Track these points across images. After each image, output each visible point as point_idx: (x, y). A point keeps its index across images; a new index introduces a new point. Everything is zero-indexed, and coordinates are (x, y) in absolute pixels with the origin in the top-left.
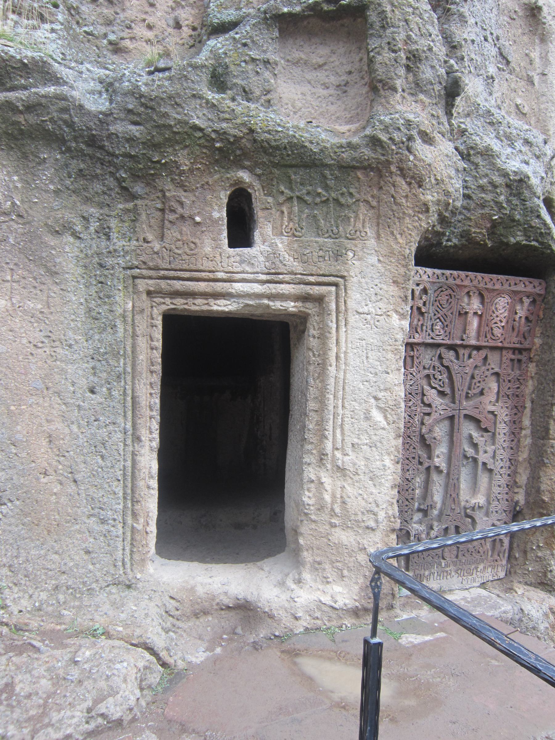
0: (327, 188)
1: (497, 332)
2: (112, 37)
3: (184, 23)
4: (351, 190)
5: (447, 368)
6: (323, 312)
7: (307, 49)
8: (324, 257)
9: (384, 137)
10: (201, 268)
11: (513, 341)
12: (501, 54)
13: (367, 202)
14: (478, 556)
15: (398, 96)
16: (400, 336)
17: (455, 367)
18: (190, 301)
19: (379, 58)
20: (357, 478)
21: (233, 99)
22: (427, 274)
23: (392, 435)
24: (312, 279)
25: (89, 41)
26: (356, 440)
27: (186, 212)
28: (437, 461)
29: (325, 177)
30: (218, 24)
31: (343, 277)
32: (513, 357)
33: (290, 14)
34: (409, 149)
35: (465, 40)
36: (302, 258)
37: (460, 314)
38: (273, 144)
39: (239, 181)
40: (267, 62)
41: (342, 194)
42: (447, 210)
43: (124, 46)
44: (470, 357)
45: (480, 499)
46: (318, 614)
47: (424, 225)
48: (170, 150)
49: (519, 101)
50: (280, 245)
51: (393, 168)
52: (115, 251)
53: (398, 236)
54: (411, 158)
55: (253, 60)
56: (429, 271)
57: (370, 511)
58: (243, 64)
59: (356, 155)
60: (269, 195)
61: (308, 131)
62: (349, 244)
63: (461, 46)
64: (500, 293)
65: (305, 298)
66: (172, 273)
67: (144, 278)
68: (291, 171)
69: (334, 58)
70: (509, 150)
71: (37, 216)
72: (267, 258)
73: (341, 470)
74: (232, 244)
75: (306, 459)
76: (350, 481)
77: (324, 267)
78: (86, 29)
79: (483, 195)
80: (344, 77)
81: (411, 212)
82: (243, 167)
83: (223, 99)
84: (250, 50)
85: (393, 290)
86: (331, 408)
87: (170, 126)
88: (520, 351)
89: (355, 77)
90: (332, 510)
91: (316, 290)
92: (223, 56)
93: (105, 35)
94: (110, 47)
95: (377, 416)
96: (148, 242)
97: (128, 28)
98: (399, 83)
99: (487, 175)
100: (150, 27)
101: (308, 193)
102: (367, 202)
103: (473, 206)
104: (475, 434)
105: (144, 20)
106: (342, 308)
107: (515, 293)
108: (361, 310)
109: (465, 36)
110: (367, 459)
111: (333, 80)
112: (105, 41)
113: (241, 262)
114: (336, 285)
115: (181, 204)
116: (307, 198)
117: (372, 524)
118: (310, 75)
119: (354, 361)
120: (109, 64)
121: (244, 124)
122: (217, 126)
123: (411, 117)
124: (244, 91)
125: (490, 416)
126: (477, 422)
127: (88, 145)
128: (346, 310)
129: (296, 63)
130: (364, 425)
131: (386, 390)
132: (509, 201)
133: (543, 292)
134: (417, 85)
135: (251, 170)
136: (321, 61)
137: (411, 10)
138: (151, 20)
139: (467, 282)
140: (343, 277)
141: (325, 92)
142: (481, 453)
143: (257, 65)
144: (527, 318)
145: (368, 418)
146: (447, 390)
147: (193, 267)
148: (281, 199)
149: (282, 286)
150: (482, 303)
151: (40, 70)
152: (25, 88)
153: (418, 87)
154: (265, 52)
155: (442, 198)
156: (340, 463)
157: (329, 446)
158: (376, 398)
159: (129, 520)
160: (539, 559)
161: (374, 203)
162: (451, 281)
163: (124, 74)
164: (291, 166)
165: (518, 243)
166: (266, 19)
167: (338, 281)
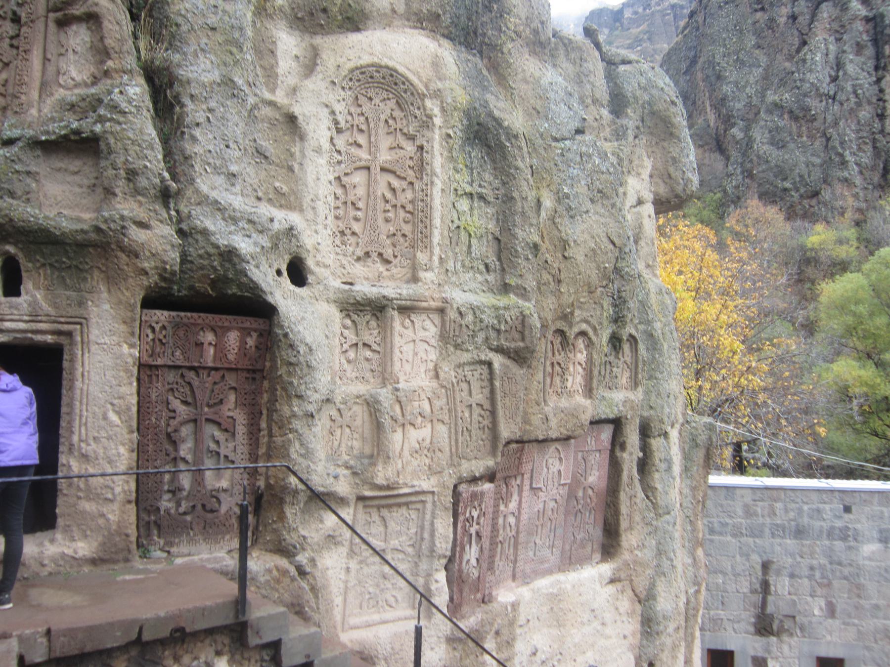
0: (69, 258)
1: (231, 357)
4: (87, 260)
5: (189, 383)
6: (72, 343)
7: (66, 161)
8: (70, 305)
9: (104, 227)
11: (245, 364)
12: (258, 152)
13: (99, 268)
14: (224, 528)
15: (118, 199)
17: (196, 383)
19: (105, 174)
22: (161, 316)
23: (125, 431)
24: (62, 320)
26: (96, 434)
28: (182, 453)
29: (67, 251)
31: (85, 319)
32: (248, 375)
33: (47, 141)
34: (124, 235)
35: (196, 154)
36: (56, 306)
37: (196, 344)
38: (27, 229)
39: (7, 252)
40: (28, 173)
41: (81, 263)
42: (166, 272)
44: (209, 375)
45: (224, 484)
46: (62, 563)
47: (146, 283)
49: (277, 184)
50: (38, 296)
51: (113, 246)
53: (125, 291)
54: (126, 240)
55: (18, 172)
56: (166, 313)
57: (107, 487)
59: (85, 237)
60: (30, 261)
61: (55, 220)
62: (87, 296)
63: (191, 157)
64: (229, 329)
65: (59, 333)
69: (86, 168)
70: (233, 228)
72: (30, 305)
73: (85, 457)
74: (7, 294)
76: (92, 464)
77: (72, 311)
80: (93, 181)
81: (132, 274)
82: (9, 243)
84: (16, 164)
85: (123, 328)
86: (78, 411)
88: (254, 371)
90: (78, 486)
91: (66, 327)
95: (113, 417)
98: (117, 191)
99: (204, 247)
101: (57, 261)
102: (99, 268)
103: (195, 268)
106: (86, 340)
107: (244, 329)
109: (196, 150)
110: (105, 448)
111: (86, 182)
113: (11, 307)
114: (81, 324)
116: (56, 265)
117: (110, 496)
118: (70, 178)
119: (94, 377)
121: (6, 215)
123: (126, 213)
125: (230, 420)
126: (219, 424)
128: (89, 342)
129: (59, 170)
130: (103, 423)
131: (120, 398)
132: (222, 266)
133: (267, 328)
134: (136, 190)
135: (15, 244)
136: (76, 170)
137: (130, 142)
139: (200, 321)
140: (85, 319)
141: (78, 190)
142: (222, 447)
144: (256, 347)
145: (105, 418)
146: (190, 400)
148: (38, 265)
149: (41, 324)
150: (216, 335)
153: (137, 192)
155: (159, 264)
156: (84, 451)
157: (75, 438)
158: (112, 404)
160: (275, 531)
161: (104, 269)
162: (185, 320)
164: (42, 243)
165: (234, 294)
166: (29, 143)
167: (82, 321)
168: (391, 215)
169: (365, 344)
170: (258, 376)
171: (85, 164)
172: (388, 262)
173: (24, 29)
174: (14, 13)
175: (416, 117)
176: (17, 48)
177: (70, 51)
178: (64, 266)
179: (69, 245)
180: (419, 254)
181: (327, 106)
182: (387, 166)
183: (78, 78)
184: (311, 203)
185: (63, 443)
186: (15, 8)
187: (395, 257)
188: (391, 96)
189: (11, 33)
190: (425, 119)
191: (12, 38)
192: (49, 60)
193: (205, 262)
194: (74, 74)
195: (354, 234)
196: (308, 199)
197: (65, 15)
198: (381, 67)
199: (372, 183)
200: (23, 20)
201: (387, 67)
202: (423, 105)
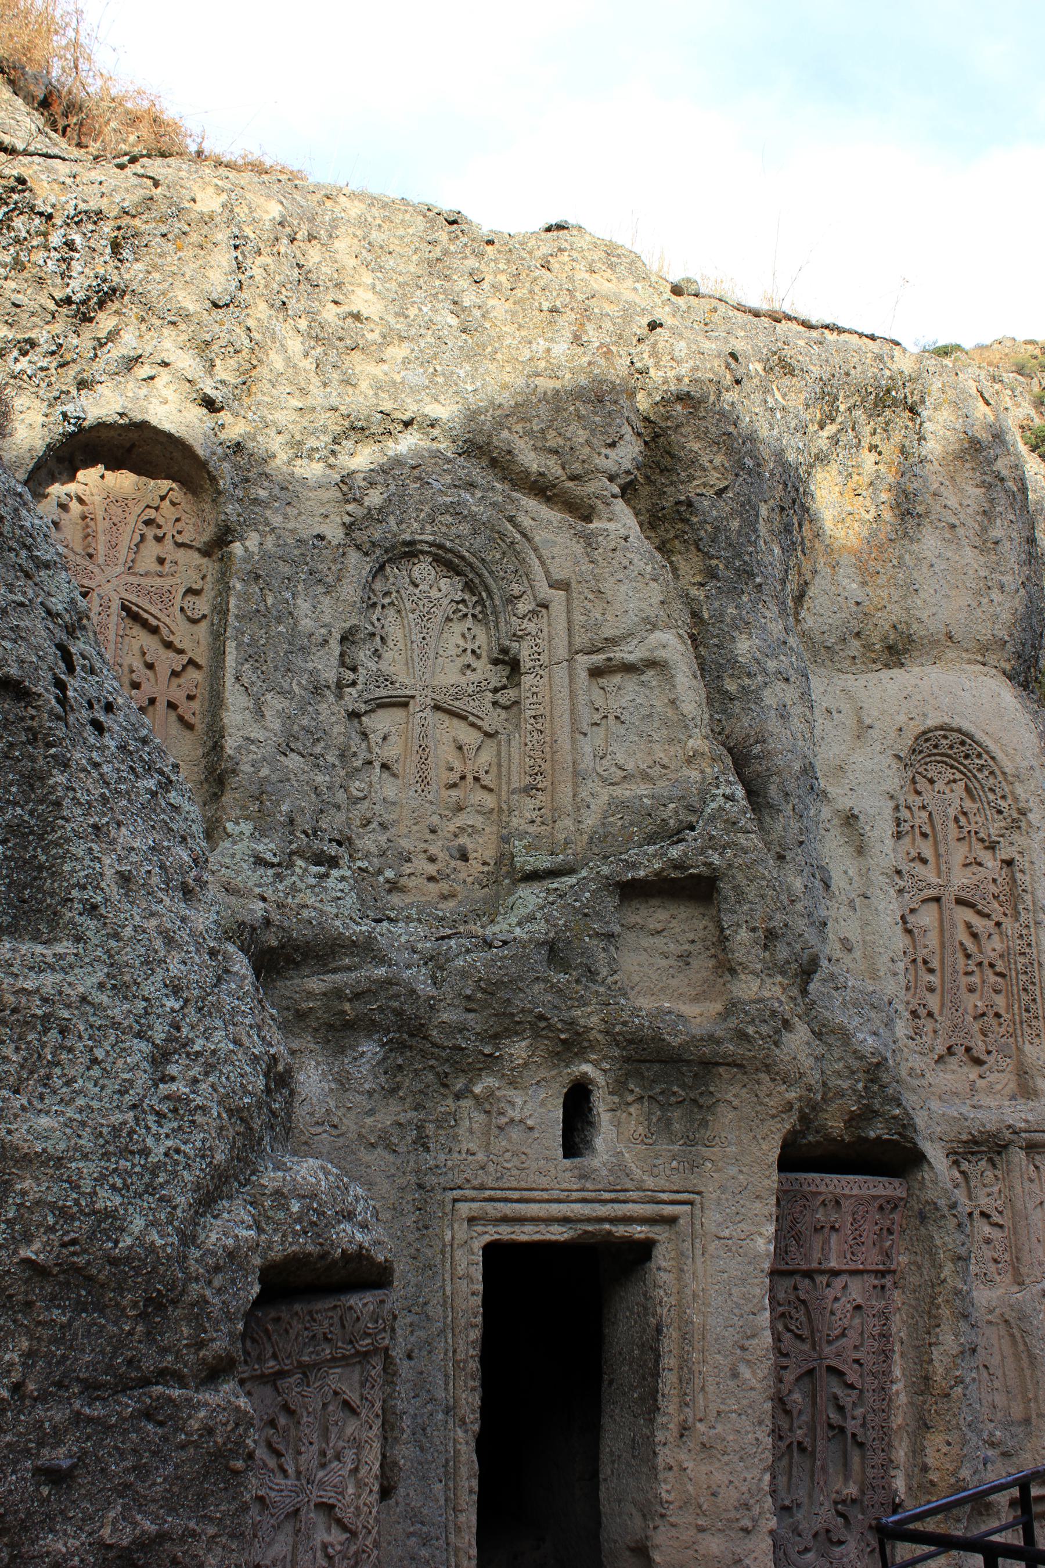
0: (683, 1086)
2: (389, 874)
7: (644, 912)
9: (750, 1030)
10: (534, 1186)
16: (767, 1266)
18: (517, 1228)
20: (726, 1458)
21: (578, 981)
24: (664, 1196)
26: (723, 1407)
27: (516, 1115)
31: (699, 1193)
32: (876, 1282)
48: (507, 1042)
52: (437, 1167)
58: (587, 939)
66: (499, 1194)
67: (466, 1200)
68: (643, 1067)
69: (674, 923)
71: (349, 1124)
75: (660, 1436)
76: (717, 1465)
78: (359, 863)
79: (839, 1082)
80: (686, 947)
83: (568, 981)
87: (513, 1015)
88: (883, 1274)
89: (699, 946)
91: (668, 1210)
96: (473, 1154)
100: (432, 860)
104: (839, 1391)
108: (722, 1235)
115: (512, 1104)
122: (565, 1016)
124: (590, 971)
127: (412, 1035)
130: (732, 1384)
135: (595, 1064)
137: (764, 883)
138: (433, 850)
139: (822, 1188)
140: (699, 1193)
141: (664, 963)
142: (849, 1419)
145: (735, 1375)
146: (805, 1333)
147: (523, 1184)
149: (630, 1206)
151: (366, 949)
152: (349, 969)
158: (743, 1348)
159: (452, 1538)
165: (879, 1138)
168: (975, 979)
169: (983, 1214)
170: (888, 1281)
171: (673, 917)
172: (978, 1062)
175: (1000, 812)
177: (611, 717)
178: (673, 1099)
179: (688, 1062)
180: (1027, 1047)
181: (892, 797)
182: (964, 894)
183: (630, 766)
184: (890, 964)
185: (665, 1427)
187: (989, 1052)
188: (958, 776)
189: (494, 683)
190: (1016, 815)
191: (496, 690)
193: (845, 1085)
194: (621, 759)
195: (930, 1014)
196: (885, 958)
197: (609, 659)
198: (952, 730)
199: (947, 926)
200: (526, 663)
201: (959, 730)
202: (1012, 793)
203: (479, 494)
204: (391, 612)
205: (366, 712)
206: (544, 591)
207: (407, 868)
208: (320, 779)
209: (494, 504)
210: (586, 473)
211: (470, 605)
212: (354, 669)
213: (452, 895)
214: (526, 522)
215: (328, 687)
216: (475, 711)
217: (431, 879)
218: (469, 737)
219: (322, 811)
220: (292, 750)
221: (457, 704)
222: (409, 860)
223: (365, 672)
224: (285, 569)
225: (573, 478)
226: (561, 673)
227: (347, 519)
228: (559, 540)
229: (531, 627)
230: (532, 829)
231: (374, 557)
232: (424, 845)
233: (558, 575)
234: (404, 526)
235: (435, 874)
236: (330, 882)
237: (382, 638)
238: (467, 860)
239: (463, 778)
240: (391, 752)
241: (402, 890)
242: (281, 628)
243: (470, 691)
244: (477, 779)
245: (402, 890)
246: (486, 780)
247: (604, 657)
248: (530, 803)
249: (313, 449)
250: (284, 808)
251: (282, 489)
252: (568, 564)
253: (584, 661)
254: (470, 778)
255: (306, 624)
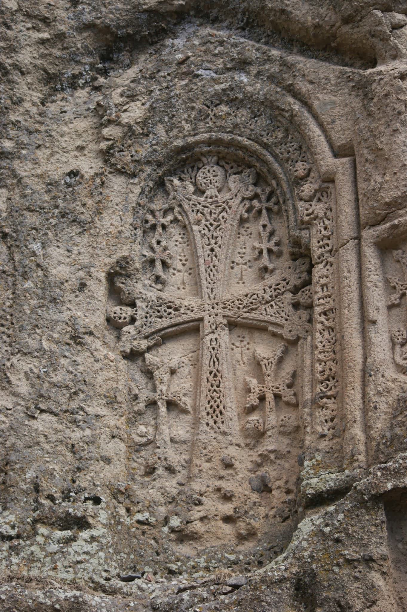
2: (175, 522)
3: (274, 485)
25: (144, 533)
30: (313, 495)
43: (192, 532)
55: (349, 562)
58: (336, 569)
78: (139, 517)
92: (309, 560)
93: (166, 521)
94: (173, 536)
97: (196, 505)
100: (227, 498)
105: (219, 490)
112: (166, 529)
120: (171, 562)
138: (227, 486)
143: (356, 568)
154: (365, 546)
163: (182, 600)
173: (319, 270)
174: (296, 243)
176: (310, 307)
186: (296, 233)
189: (294, 281)
191: (295, 290)
192: (374, 322)
197: (394, 227)
200: (316, 252)
203: (254, 70)
204: (175, 231)
205: (149, 349)
206: (327, 160)
207: (196, 513)
208: (76, 435)
209: (271, 78)
210: (357, 11)
211: (263, 198)
212: (133, 305)
213: (251, 534)
214: (303, 87)
215: (91, 333)
216: (272, 319)
217: (227, 519)
218: (265, 350)
219: (79, 469)
220: (42, 411)
221: (252, 315)
222: (200, 503)
223: (144, 305)
224: (32, 219)
225: (347, 21)
226: (349, 256)
227: (104, 145)
228: (338, 99)
229: (318, 208)
230: (324, 445)
231: (143, 175)
232: (218, 483)
233: (340, 139)
234: (175, 132)
235: (231, 512)
236: (75, 546)
237: (164, 264)
238: (270, 491)
239: (262, 398)
240: (180, 387)
241: (194, 537)
242: (28, 284)
243: (267, 297)
244: (277, 397)
245: (194, 537)
246: (288, 395)
247: (388, 225)
248: (321, 415)
249: (74, 77)
250: (30, 474)
251: (30, 133)
252: (349, 124)
253: (368, 234)
254: (270, 397)
255: (60, 272)
